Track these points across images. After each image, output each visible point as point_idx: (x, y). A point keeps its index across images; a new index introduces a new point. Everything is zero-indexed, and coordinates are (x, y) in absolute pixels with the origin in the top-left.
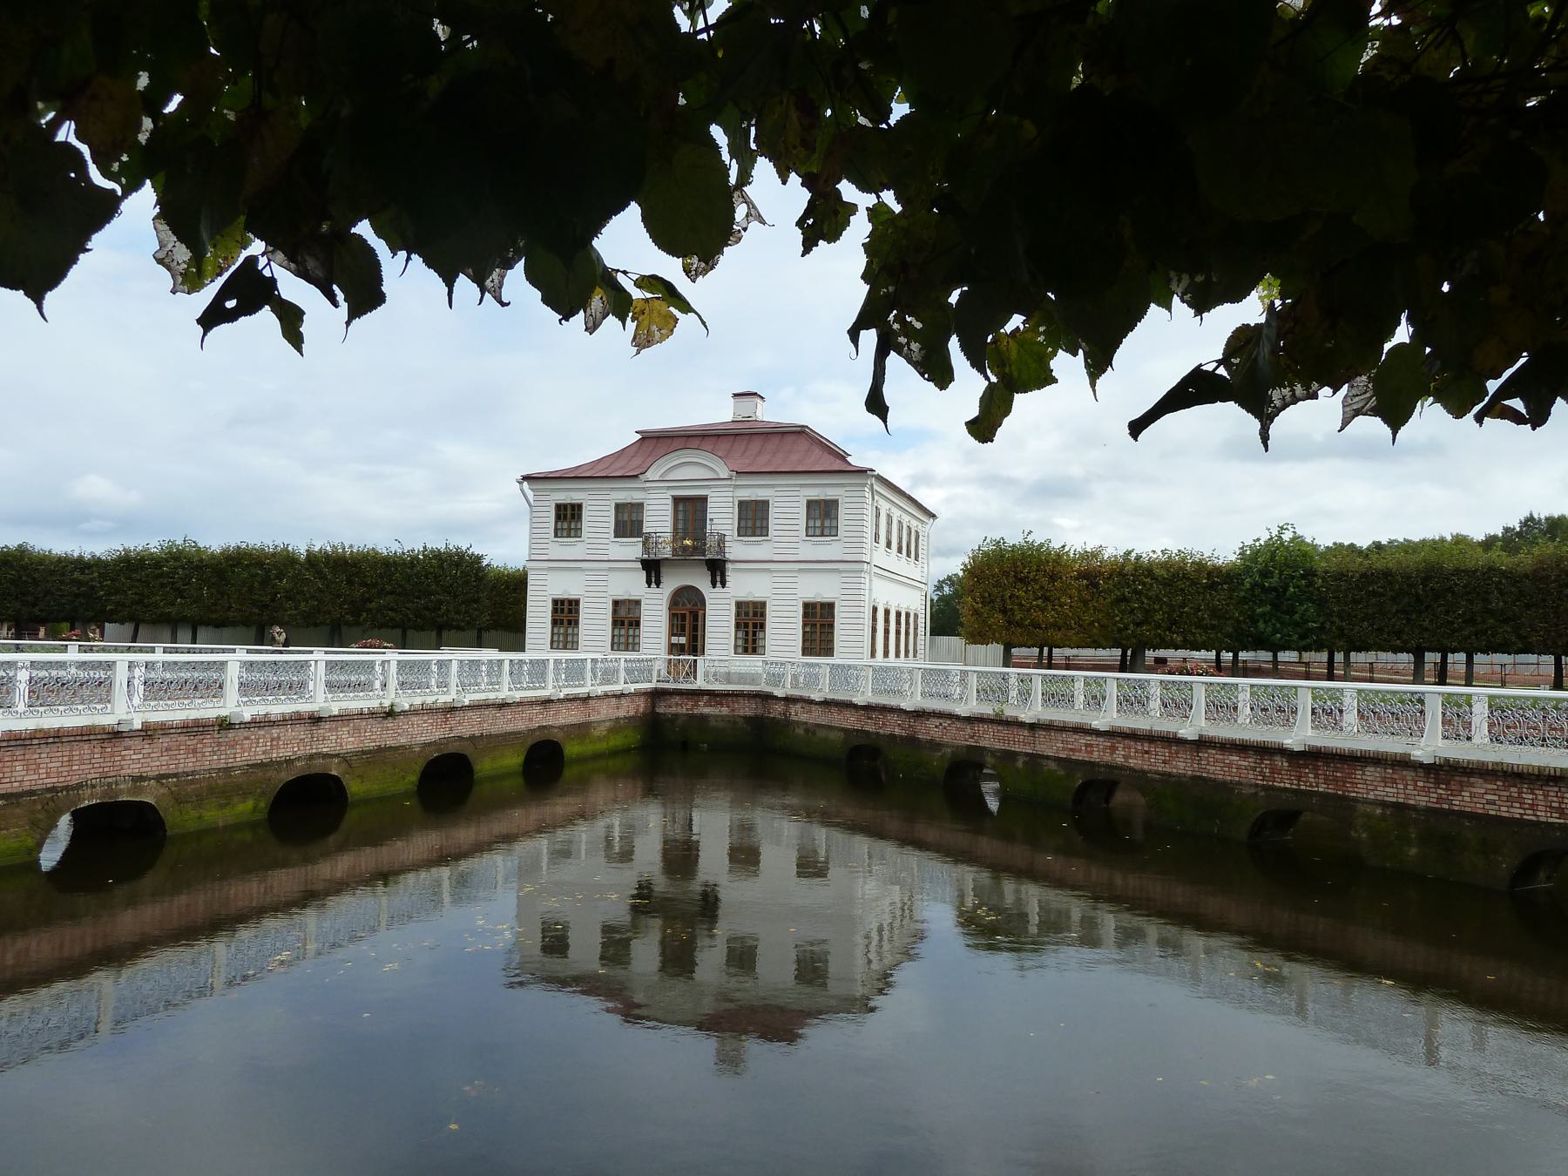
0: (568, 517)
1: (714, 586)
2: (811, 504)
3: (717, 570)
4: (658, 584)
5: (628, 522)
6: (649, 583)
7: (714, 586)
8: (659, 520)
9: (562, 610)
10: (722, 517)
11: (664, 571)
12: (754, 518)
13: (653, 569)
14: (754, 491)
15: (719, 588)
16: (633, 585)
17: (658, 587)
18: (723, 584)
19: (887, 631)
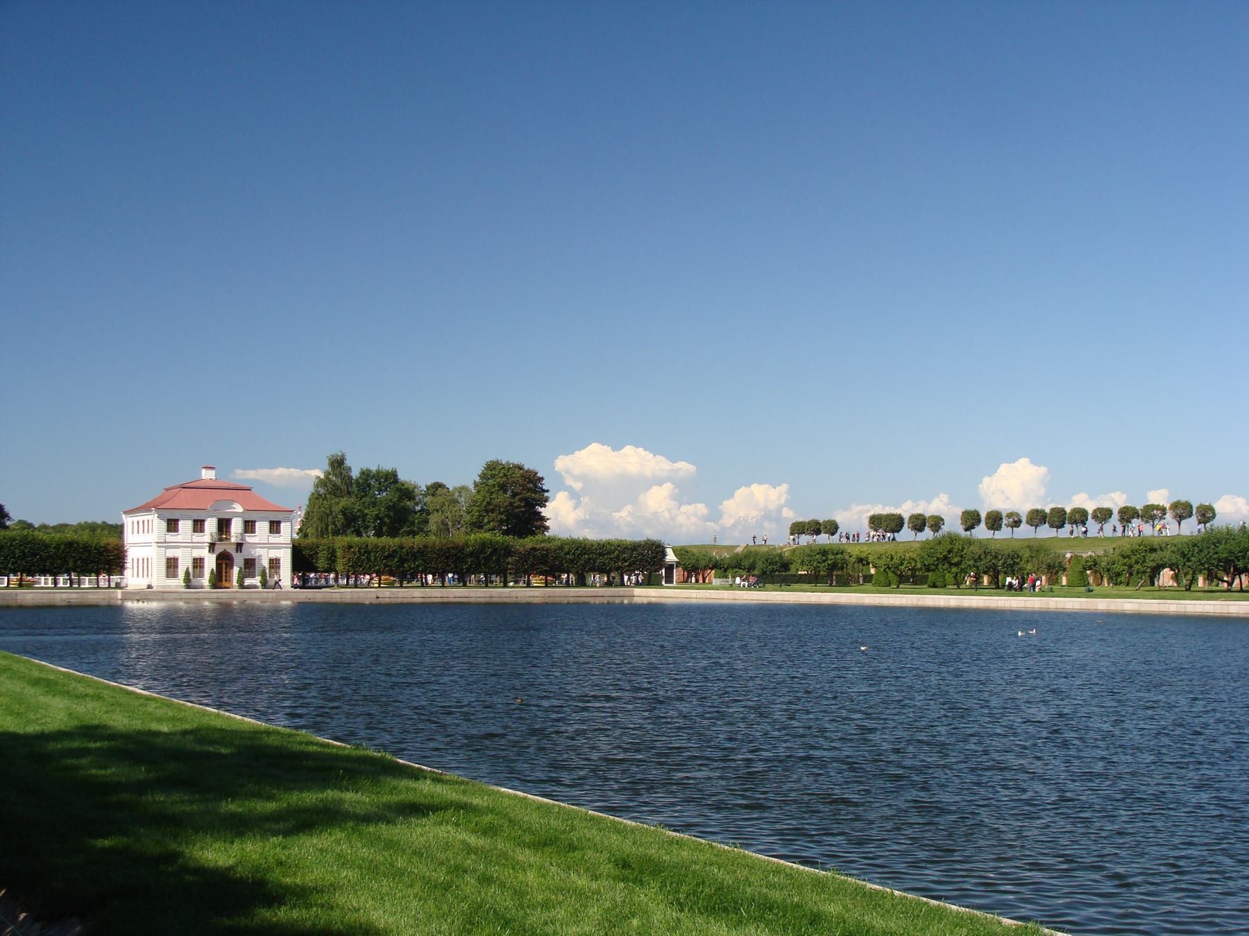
0: (172, 525)
1: (237, 552)
2: (272, 523)
3: (239, 546)
4: (213, 552)
5: (198, 526)
6: (209, 551)
7: (237, 552)
8: (211, 525)
9: (171, 563)
10: (236, 527)
11: (216, 547)
12: (249, 526)
13: (212, 547)
14: (250, 518)
15: (239, 553)
16: (204, 553)
17: (213, 552)
18: (241, 552)
19: (143, 567)
